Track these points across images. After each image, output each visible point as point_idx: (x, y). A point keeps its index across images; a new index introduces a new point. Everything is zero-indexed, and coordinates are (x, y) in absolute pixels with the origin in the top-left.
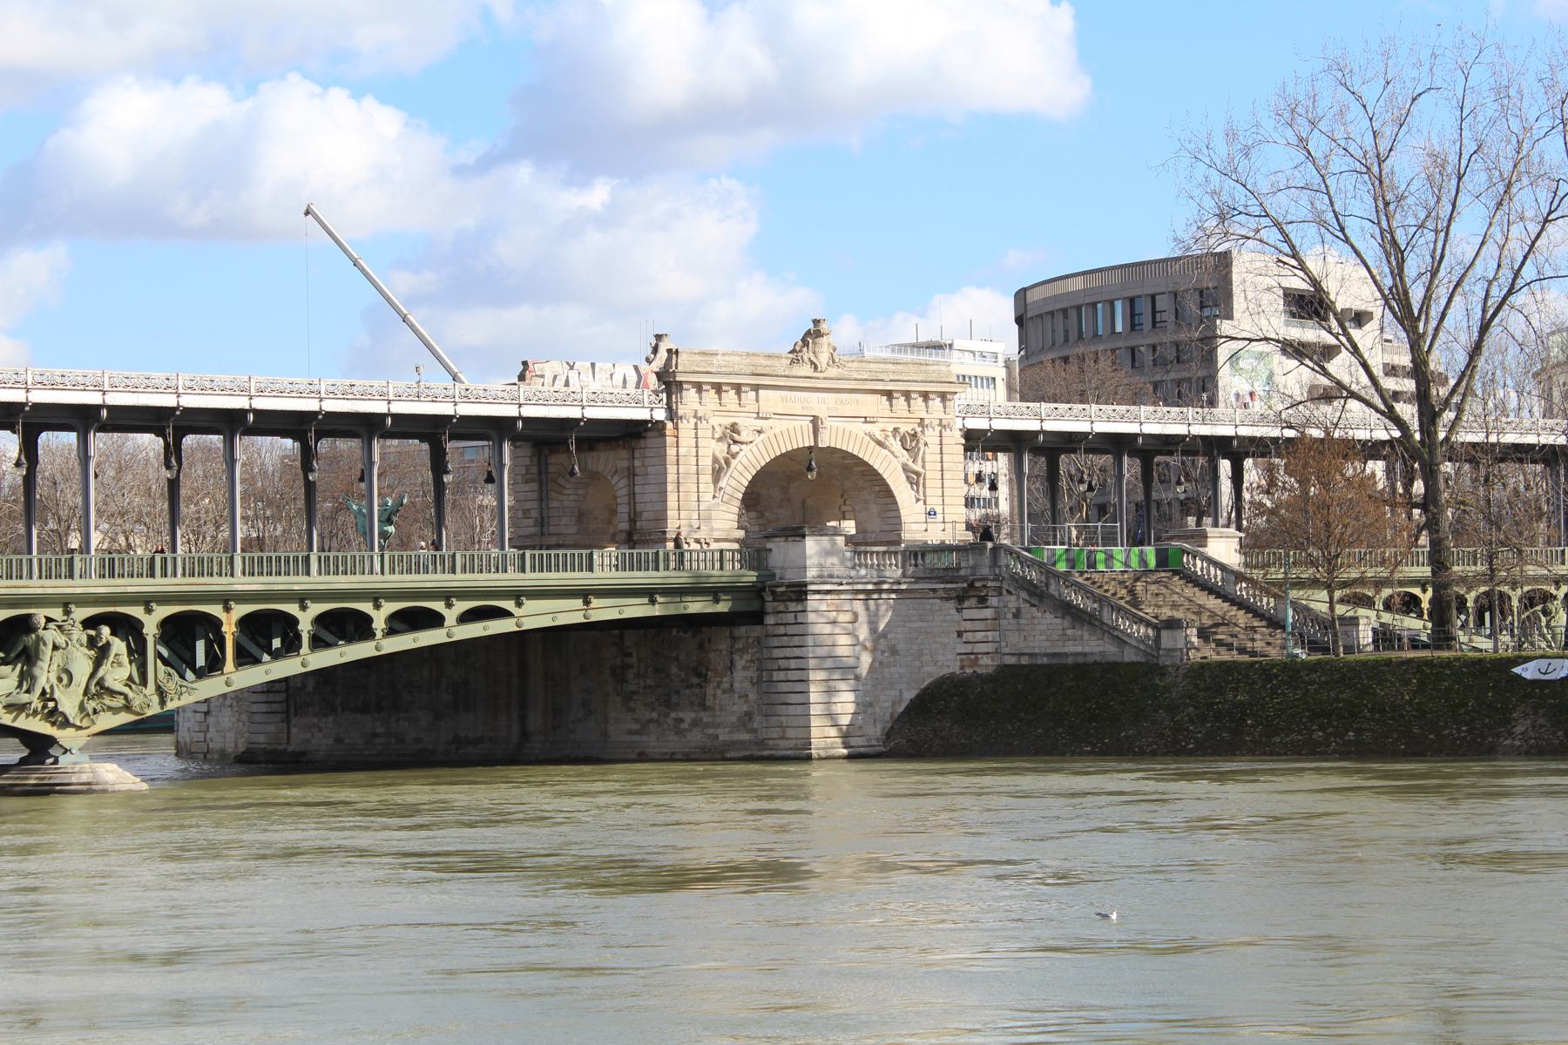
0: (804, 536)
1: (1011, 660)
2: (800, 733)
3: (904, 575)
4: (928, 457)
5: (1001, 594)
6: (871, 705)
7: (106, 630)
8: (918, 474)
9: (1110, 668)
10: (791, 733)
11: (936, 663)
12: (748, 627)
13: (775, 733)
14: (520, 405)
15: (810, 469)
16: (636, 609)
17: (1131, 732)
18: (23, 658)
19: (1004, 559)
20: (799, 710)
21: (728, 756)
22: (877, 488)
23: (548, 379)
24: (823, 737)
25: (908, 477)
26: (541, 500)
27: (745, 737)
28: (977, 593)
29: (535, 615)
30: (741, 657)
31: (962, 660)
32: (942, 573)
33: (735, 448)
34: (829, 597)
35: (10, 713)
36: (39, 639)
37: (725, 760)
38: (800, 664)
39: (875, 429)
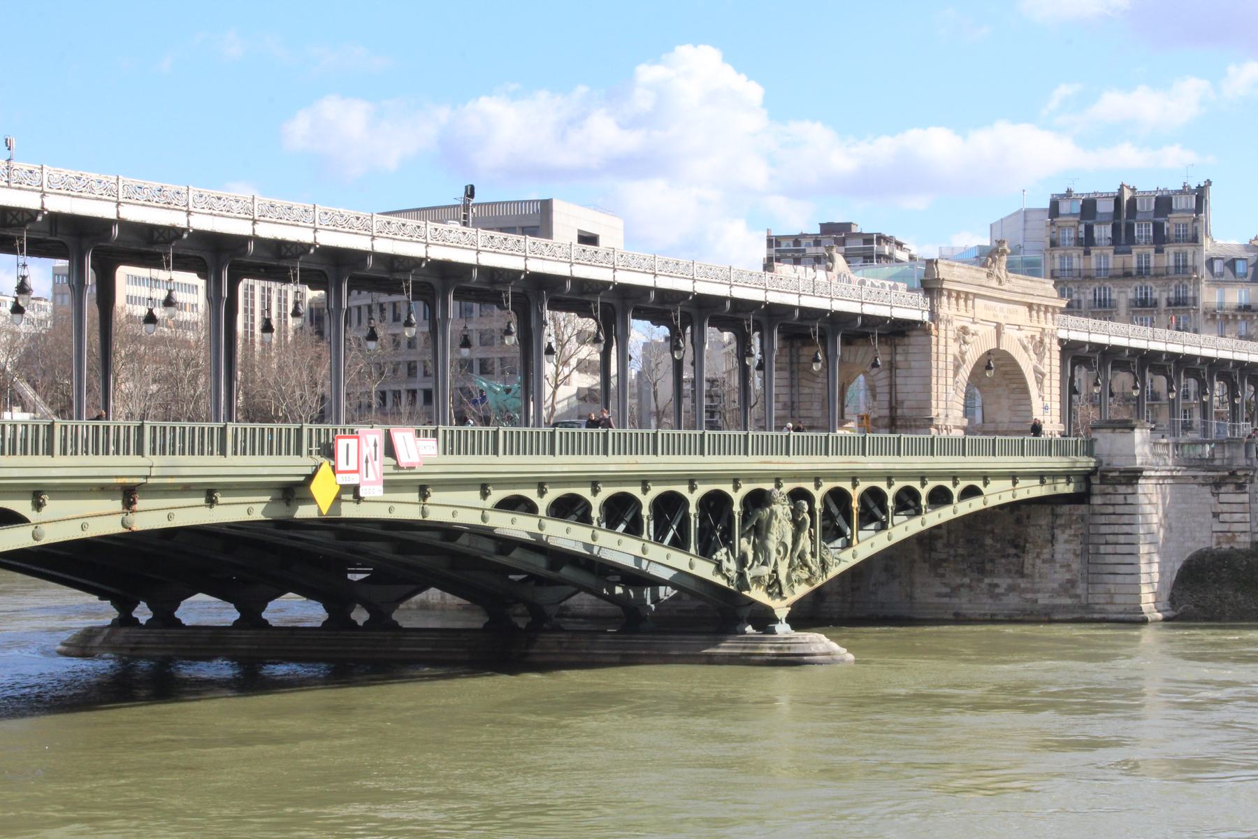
0: (1132, 428)
2: (1130, 599)
10: (1118, 599)
12: (1072, 506)
18: (753, 532)
20: (1129, 579)
24: (1148, 600)
26: (792, 386)
27: (1068, 601)
28: (1235, 481)
29: (997, 494)
30: (1064, 532)
31: (1218, 537)
32: (1198, 463)
33: (964, 347)
37: (1051, 621)
39: (1022, 335)
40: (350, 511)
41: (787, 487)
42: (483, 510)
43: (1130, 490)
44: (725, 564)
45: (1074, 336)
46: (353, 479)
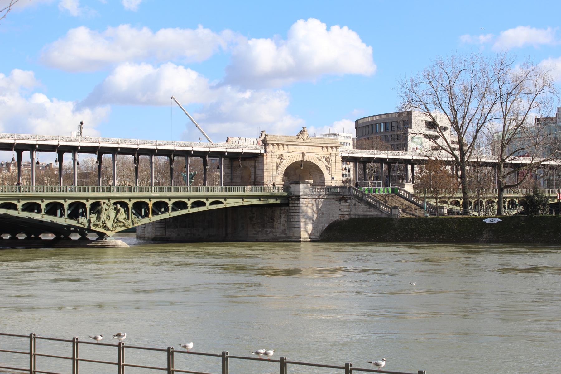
0: (299, 184)
1: (353, 217)
2: (298, 235)
3: (325, 194)
4: (332, 164)
5: (351, 199)
6: (316, 228)
7: (119, 206)
8: (329, 168)
9: (380, 219)
10: (296, 235)
11: (333, 217)
13: (291, 235)
14: (226, 149)
15: (301, 166)
16: (256, 202)
17: (384, 236)
19: (352, 190)
20: (298, 229)
21: (279, 240)
22: (319, 171)
23: (234, 142)
24: (304, 236)
25: (327, 169)
26: (231, 173)
27: (283, 235)
29: (230, 203)
32: (335, 194)
33: (282, 160)
34: (306, 199)
35: (94, 227)
36: (102, 208)
37: (278, 241)
39: (319, 156)
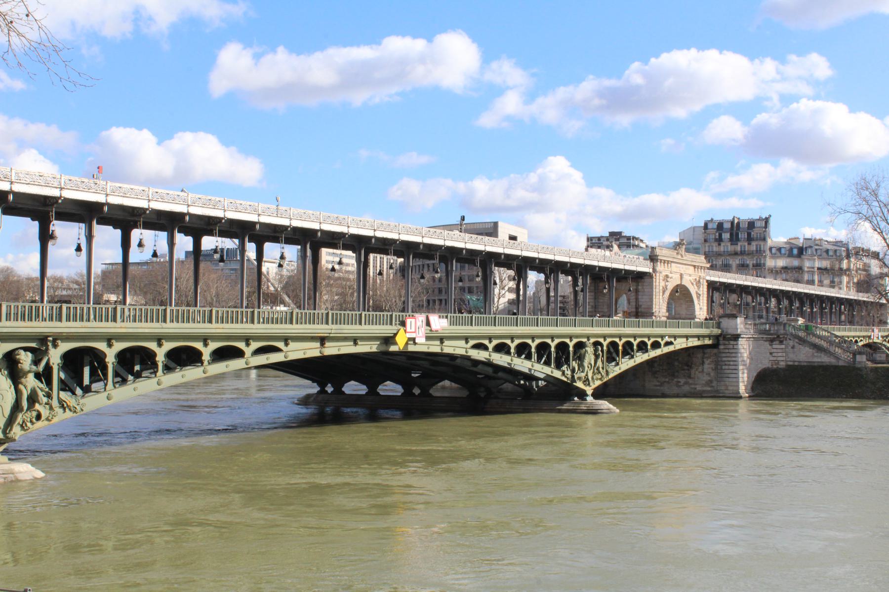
0: (737, 317)
1: (791, 363)
2: (735, 388)
5: (786, 340)
10: (730, 388)
11: (761, 363)
13: (723, 388)
15: (677, 292)
17: (860, 391)
20: (735, 380)
24: (742, 389)
26: (595, 299)
27: (709, 389)
29: (680, 344)
32: (764, 332)
36: (586, 351)
38: (735, 363)
39: (691, 278)
40: (412, 348)
41: (592, 340)
42: (466, 348)
43: (735, 343)
44: (566, 372)
45: (713, 279)
46: (413, 336)
